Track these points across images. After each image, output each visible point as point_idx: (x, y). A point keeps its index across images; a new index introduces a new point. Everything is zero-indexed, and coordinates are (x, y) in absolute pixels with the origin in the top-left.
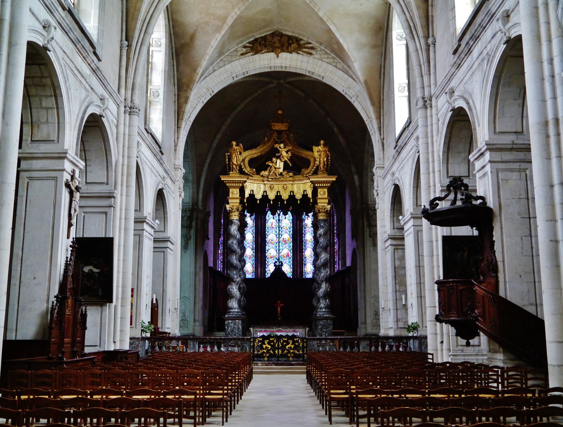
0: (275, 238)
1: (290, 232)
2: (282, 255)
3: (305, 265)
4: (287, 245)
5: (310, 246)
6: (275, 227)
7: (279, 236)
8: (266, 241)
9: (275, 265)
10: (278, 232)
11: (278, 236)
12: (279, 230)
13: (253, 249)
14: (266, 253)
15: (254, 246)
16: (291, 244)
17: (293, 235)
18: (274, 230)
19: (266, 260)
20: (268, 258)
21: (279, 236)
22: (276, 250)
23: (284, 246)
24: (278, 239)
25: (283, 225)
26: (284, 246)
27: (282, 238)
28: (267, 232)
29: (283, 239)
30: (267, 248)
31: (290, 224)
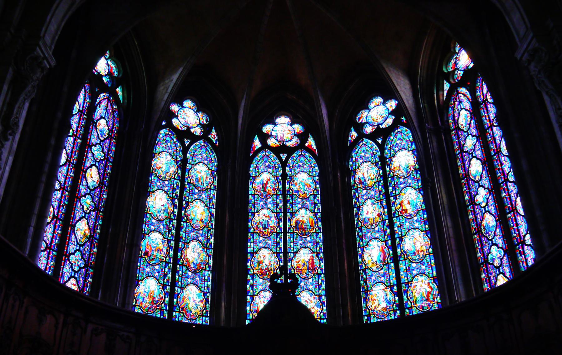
0: (273, 222)
1: (316, 205)
2: (295, 266)
3: (367, 292)
4: (309, 239)
5: (377, 235)
6: (272, 192)
7: (285, 216)
8: (247, 230)
9: (273, 287)
10: (281, 205)
11: (281, 216)
12: (285, 202)
13: (205, 248)
14: (247, 260)
15: (212, 240)
16: (320, 235)
17: (324, 211)
18: (269, 200)
19: (247, 282)
20: (252, 276)
21: (285, 216)
22: (278, 254)
23: (301, 242)
24: (281, 224)
25: (295, 189)
26: (301, 242)
27: (294, 220)
28: (250, 206)
29: (297, 223)
30: (251, 246)
31: (313, 186)
